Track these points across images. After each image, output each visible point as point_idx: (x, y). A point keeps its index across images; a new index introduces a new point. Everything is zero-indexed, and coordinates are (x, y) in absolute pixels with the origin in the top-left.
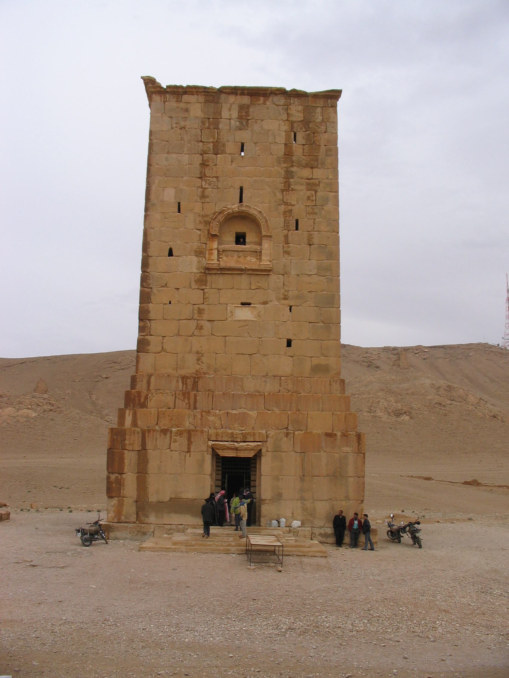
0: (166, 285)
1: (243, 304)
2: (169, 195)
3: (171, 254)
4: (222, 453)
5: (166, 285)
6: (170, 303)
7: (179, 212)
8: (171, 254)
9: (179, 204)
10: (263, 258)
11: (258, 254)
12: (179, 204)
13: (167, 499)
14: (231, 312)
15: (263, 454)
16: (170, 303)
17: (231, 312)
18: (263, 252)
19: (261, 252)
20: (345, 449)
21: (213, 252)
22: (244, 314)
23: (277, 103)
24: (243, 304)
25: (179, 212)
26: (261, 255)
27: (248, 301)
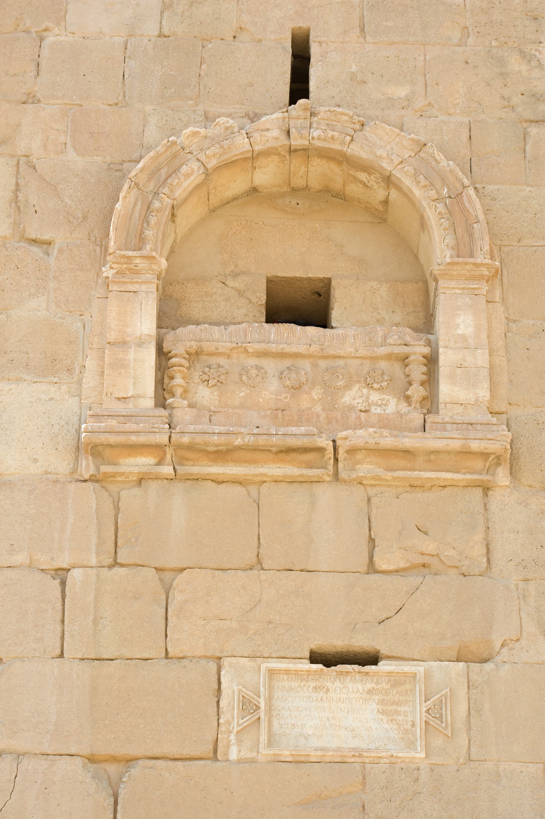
10: (446, 389)
11: (418, 371)
14: (248, 706)
19: (431, 361)
21: (132, 355)
24: (325, 659)
27: (361, 643)
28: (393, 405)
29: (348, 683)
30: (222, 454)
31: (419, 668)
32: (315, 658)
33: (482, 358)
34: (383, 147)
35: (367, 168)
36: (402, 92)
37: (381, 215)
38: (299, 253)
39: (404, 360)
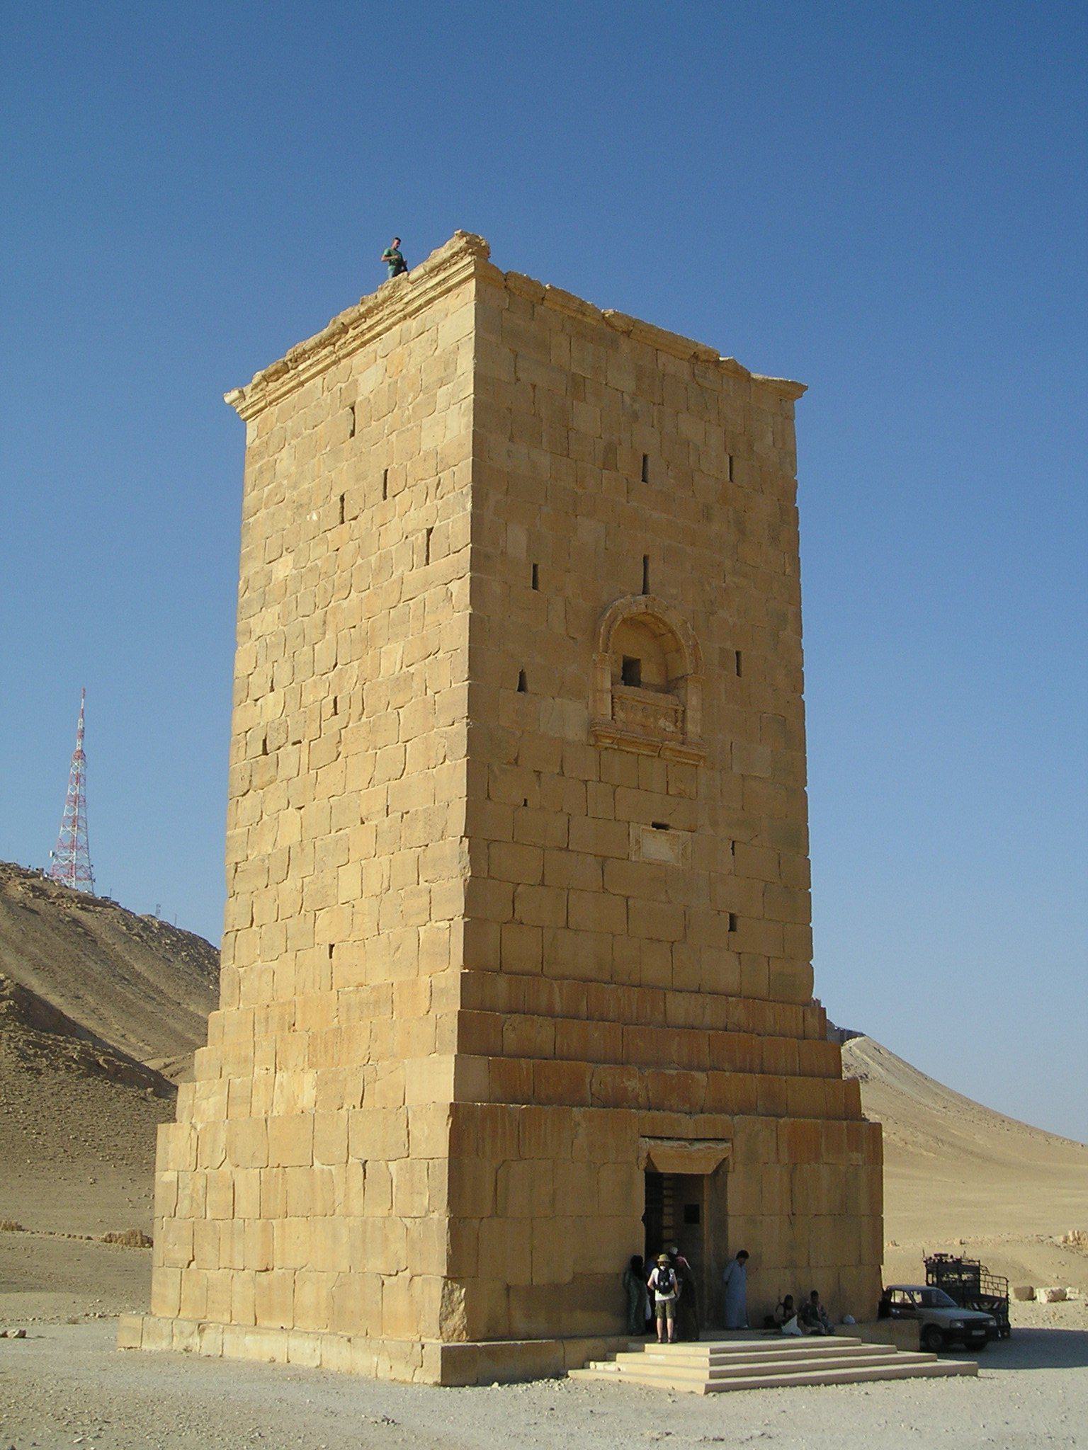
0: (516, 760)
1: (657, 826)
2: (517, 540)
3: (522, 688)
4: (662, 1168)
5: (516, 760)
6: (525, 805)
7: (535, 587)
8: (522, 688)
9: (535, 567)
10: (690, 727)
11: (680, 716)
12: (535, 567)
13: (568, 1278)
15: (731, 1169)
16: (525, 805)
17: (638, 842)
18: (689, 713)
20: (855, 1155)
22: (658, 848)
23: (700, 380)
25: (535, 587)
26: (683, 721)
27: (665, 821)
28: (672, 728)
29: (661, 836)
30: (633, 743)
31: (679, 833)
32: (654, 825)
33: (699, 715)
34: (674, 619)
35: (665, 624)
36: (674, 591)
37: (656, 636)
38: (635, 646)
39: (676, 711)
